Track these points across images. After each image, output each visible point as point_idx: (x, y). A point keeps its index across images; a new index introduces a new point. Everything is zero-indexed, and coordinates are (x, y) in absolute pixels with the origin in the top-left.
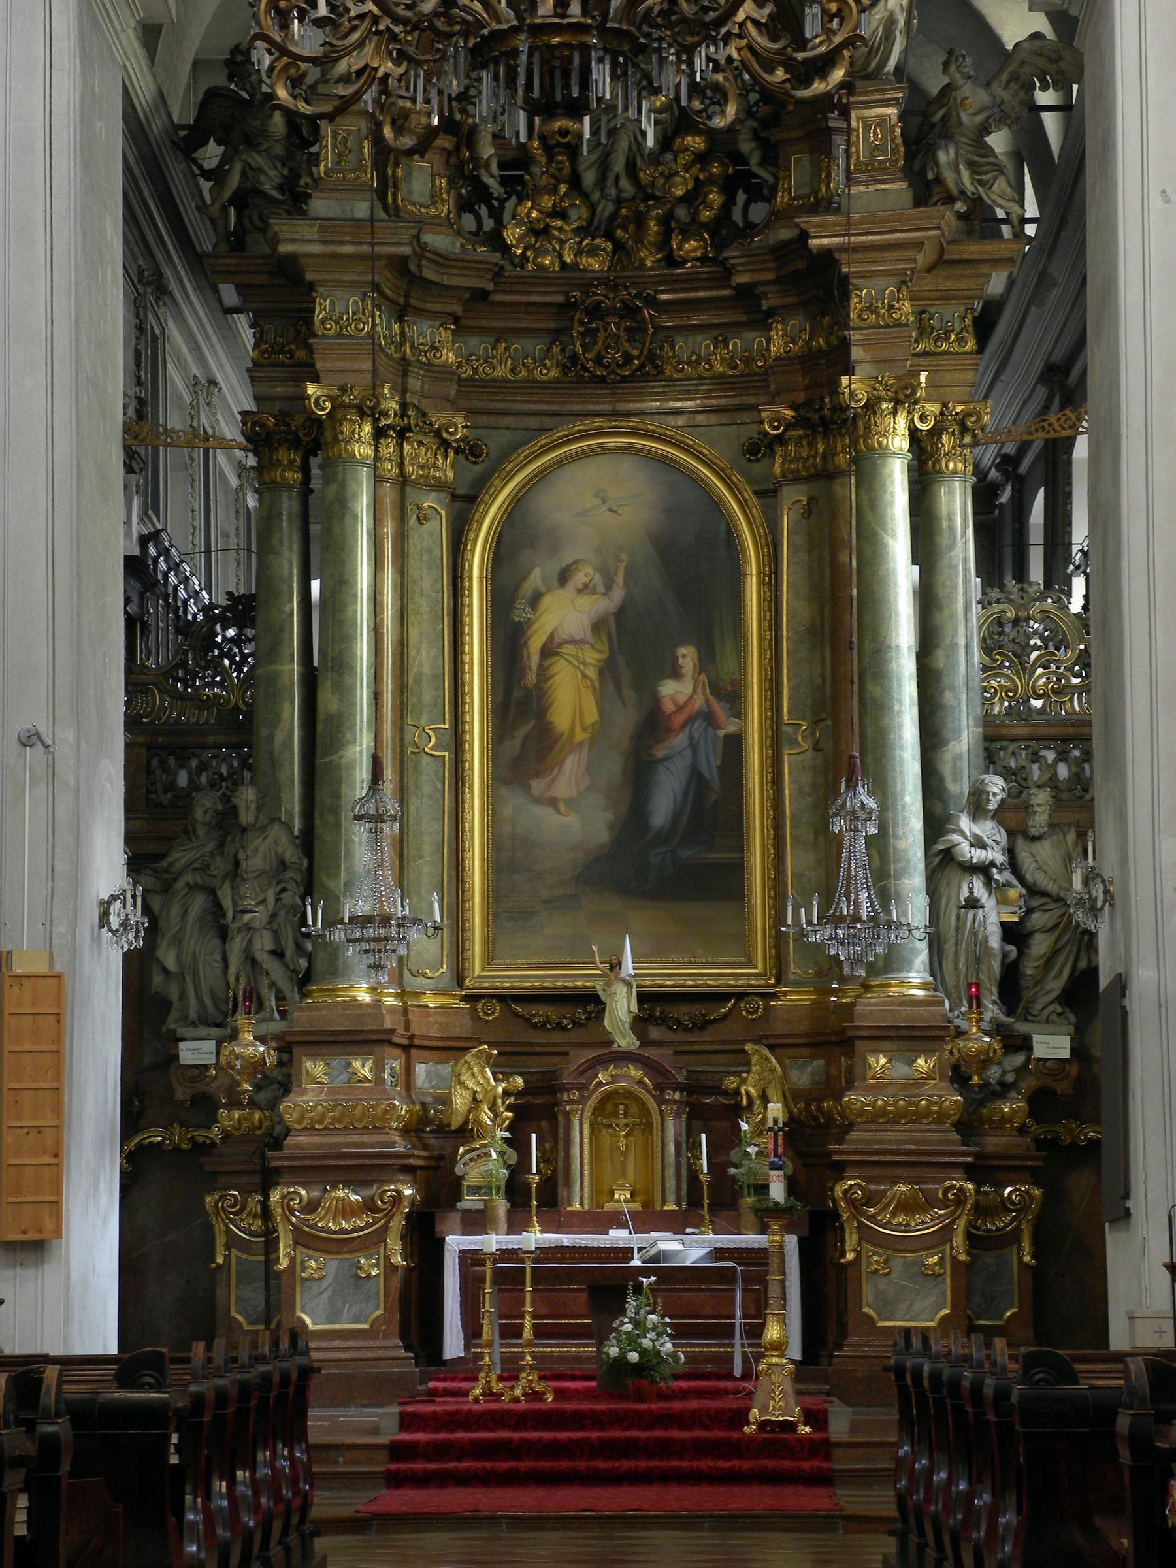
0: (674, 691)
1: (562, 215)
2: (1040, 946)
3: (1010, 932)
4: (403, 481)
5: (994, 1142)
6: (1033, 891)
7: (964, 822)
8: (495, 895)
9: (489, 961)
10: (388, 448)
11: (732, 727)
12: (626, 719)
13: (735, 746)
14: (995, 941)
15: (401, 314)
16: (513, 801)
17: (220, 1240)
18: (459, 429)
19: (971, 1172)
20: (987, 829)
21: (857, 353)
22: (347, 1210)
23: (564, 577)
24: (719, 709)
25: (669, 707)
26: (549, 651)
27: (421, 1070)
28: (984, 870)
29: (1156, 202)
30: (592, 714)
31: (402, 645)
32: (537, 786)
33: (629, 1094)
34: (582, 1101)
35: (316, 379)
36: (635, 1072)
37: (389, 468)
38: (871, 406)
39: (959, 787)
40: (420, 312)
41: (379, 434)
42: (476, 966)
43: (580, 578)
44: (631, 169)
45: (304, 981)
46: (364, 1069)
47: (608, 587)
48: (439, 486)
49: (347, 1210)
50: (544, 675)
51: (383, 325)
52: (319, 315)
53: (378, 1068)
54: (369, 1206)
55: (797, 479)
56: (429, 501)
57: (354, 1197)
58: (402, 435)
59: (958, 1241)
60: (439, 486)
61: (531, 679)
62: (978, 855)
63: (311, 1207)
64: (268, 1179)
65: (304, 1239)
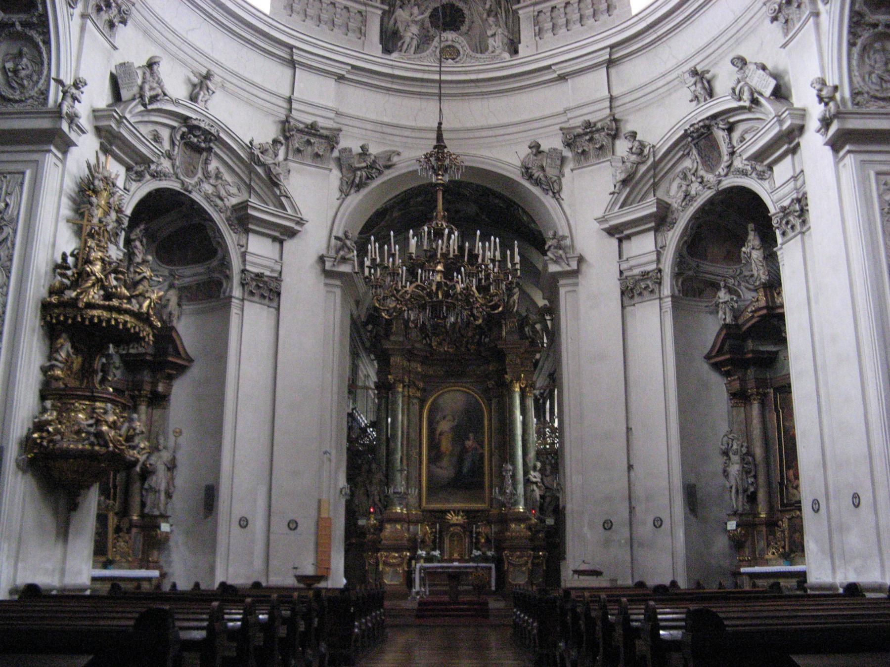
0: (469, 443)
1: (444, 340)
2: (548, 500)
3: (542, 497)
4: (409, 396)
5: (537, 543)
6: (547, 488)
7: (532, 473)
8: (429, 489)
9: (427, 503)
10: (406, 390)
11: (481, 451)
12: (458, 448)
13: (482, 456)
14: (538, 498)
15: (409, 361)
16: (433, 467)
17: (367, 564)
18: (421, 385)
19: (533, 549)
20: (537, 474)
21: (508, 370)
22: (395, 558)
23: (444, 418)
24: (478, 447)
25: (467, 447)
26: (440, 434)
27: (411, 527)
28: (536, 483)
29: (569, 340)
30: (451, 448)
31: (408, 432)
32: (438, 464)
33: (457, 533)
34: (447, 534)
35: (390, 374)
36: (459, 528)
37: (406, 393)
38: (512, 381)
39: (531, 465)
40: (415, 361)
41: (404, 386)
42: (424, 504)
43: (448, 418)
44: (460, 331)
45: (385, 507)
46: (399, 527)
47: (454, 419)
48: (416, 398)
49: (395, 558)
50: (440, 441)
51: (405, 363)
52: (391, 361)
53: (402, 527)
54: (400, 557)
55: (495, 397)
56: (415, 401)
57: (396, 555)
58: (409, 387)
59: (529, 565)
60: (416, 398)
61: (437, 441)
62: (534, 480)
63: (387, 557)
64: (378, 550)
65: (386, 564)
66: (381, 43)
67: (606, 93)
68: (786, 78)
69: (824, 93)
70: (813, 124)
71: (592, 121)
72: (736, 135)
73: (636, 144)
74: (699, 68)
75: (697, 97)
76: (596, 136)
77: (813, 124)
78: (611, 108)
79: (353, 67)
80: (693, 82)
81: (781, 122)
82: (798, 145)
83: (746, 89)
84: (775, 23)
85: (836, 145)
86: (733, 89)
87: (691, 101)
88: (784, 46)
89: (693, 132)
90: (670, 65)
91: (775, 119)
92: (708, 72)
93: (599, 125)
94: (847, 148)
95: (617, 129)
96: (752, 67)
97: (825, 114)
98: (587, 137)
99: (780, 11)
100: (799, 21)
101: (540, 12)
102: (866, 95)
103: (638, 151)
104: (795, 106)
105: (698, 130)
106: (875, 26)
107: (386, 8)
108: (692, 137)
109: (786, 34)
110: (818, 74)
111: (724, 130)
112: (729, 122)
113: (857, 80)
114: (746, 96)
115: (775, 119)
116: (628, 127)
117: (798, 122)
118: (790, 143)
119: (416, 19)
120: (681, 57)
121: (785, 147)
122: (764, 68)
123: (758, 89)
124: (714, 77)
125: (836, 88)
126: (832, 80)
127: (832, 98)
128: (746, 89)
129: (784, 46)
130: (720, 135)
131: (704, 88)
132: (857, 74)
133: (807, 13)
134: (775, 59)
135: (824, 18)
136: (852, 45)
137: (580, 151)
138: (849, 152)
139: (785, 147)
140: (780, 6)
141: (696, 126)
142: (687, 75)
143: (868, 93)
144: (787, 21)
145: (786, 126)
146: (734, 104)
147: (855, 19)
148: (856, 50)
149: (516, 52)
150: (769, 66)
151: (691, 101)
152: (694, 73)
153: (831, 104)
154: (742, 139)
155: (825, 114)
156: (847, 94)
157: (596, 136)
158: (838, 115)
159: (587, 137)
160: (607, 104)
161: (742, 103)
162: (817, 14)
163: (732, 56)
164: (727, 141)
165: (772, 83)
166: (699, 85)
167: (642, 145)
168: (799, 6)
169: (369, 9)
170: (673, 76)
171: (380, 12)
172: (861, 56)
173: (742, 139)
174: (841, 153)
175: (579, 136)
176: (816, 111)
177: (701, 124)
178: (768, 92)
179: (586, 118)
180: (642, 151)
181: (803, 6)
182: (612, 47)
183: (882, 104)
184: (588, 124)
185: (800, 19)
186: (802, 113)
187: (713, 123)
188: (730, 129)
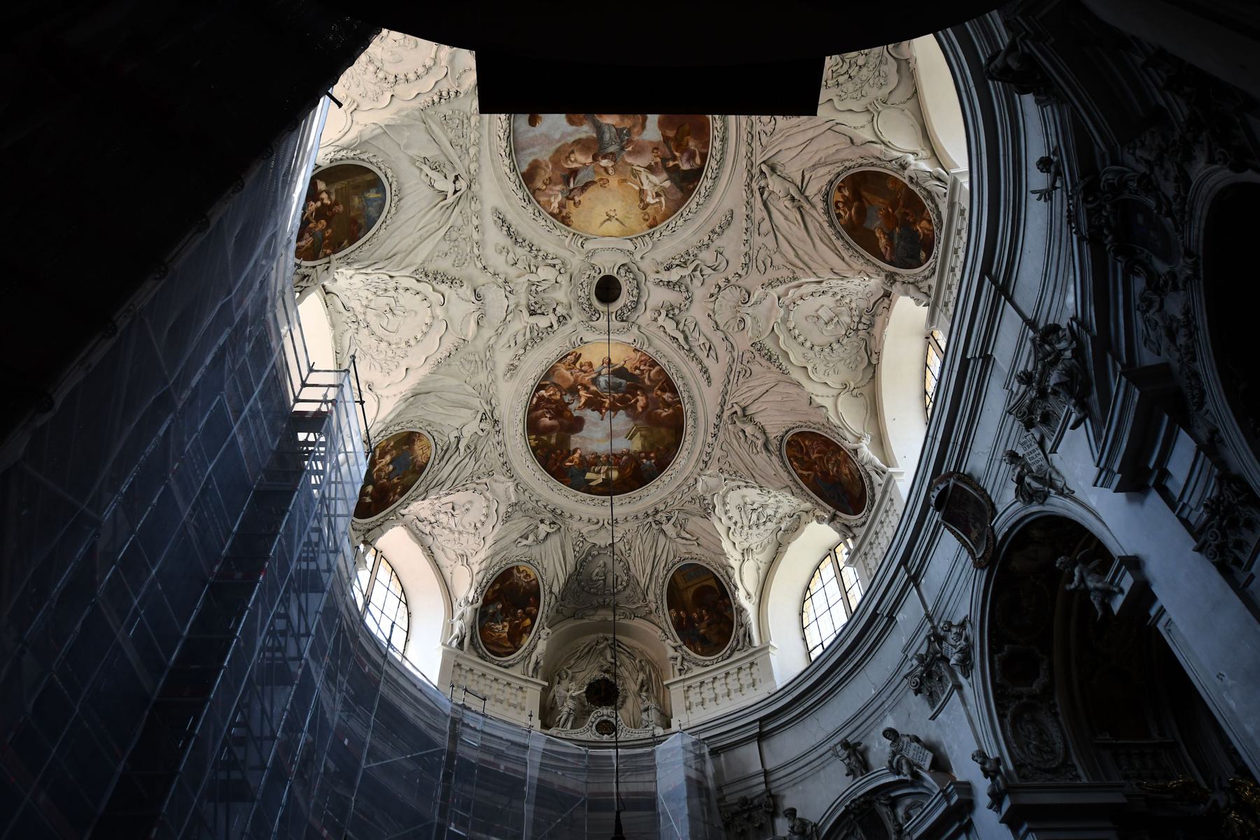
66: (540, 719)
67: (760, 768)
68: (942, 749)
69: (987, 766)
70: (983, 798)
71: (749, 797)
72: (900, 812)
73: (797, 823)
74: (849, 739)
75: (852, 770)
76: (754, 813)
77: (983, 798)
78: (766, 783)
79: (513, 743)
80: (845, 755)
81: (947, 797)
82: (970, 822)
83: (904, 761)
84: (919, 695)
85: (1012, 821)
86: (891, 762)
87: (847, 775)
88: (933, 718)
89: (854, 808)
90: (821, 736)
91: (941, 794)
92: (859, 744)
93: (756, 802)
94: (1026, 826)
95: (776, 806)
96: (906, 740)
97: (994, 789)
98: (746, 816)
99: (922, 684)
100: (943, 693)
101: (689, 687)
102: (1029, 767)
103: (800, 830)
104: (958, 779)
105: (859, 806)
106: (1019, 697)
107: (546, 684)
108: (854, 814)
109: (933, 706)
110: (976, 748)
111: (886, 805)
112: (890, 797)
113: (1016, 751)
114: (905, 769)
115: (941, 794)
116: (788, 803)
117: (965, 797)
118: (961, 820)
119: (574, 695)
120: (830, 729)
121: (957, 825)
122: (917, 740)
123: (916, 762)
124: (866, 749)
125: (998, 761)
126: (992, 753)
127: (998, 772)
128: (904, 761)
129: (933, 718)
130: (884, 811)
131: (858, 761)
132: (1015, 745)
133: (951, 685)
134: (928, 731)
135: (967, 690)
136: (1001, 717)
137: (739, 831)
138: (1029, 830)
139: (957, 825)
140: (921, 678)
141: (857, 802)
142: (839, 748)
143: (1031, 765)
144: (931, 695)
145: (953, 802)
146: (892, 779)
147: (999, 691)
148: (1008, 720)
149: (669, 726)
150: (922, 738)
151: (847, 775)
152: (845, 745)
153: (998, 778)
154: (908, 817)
155: (994, 789)
156: (1010, 767)
157: (754, 813)
158: (1010, 790)
159: (746, 816)
160: (762, 779)
161: (902, 777)
162: (959, 687)
163: (881, 731)
164: (892, 817)
165: (930, 756)
166: (853, 758)
167: (803, 823)
168: (940, 680)
169: (530, 685)
170: (826, 748)
171: (540, 688)
172: (1013, 726)
173: (908, 817)
174: (1022, 832)
175: (737, 814)
176: (982, 786)
177: (862, 799)
178: (927, 765)
179: (743, 794)
180: (804, 831)
181: (944, 679)
182: (761, 720)
183: (1049, 776)
184: (744, 801)
185: (943, 692)
186: (968, 787)
187: (874, 798)
188: (894, 803)
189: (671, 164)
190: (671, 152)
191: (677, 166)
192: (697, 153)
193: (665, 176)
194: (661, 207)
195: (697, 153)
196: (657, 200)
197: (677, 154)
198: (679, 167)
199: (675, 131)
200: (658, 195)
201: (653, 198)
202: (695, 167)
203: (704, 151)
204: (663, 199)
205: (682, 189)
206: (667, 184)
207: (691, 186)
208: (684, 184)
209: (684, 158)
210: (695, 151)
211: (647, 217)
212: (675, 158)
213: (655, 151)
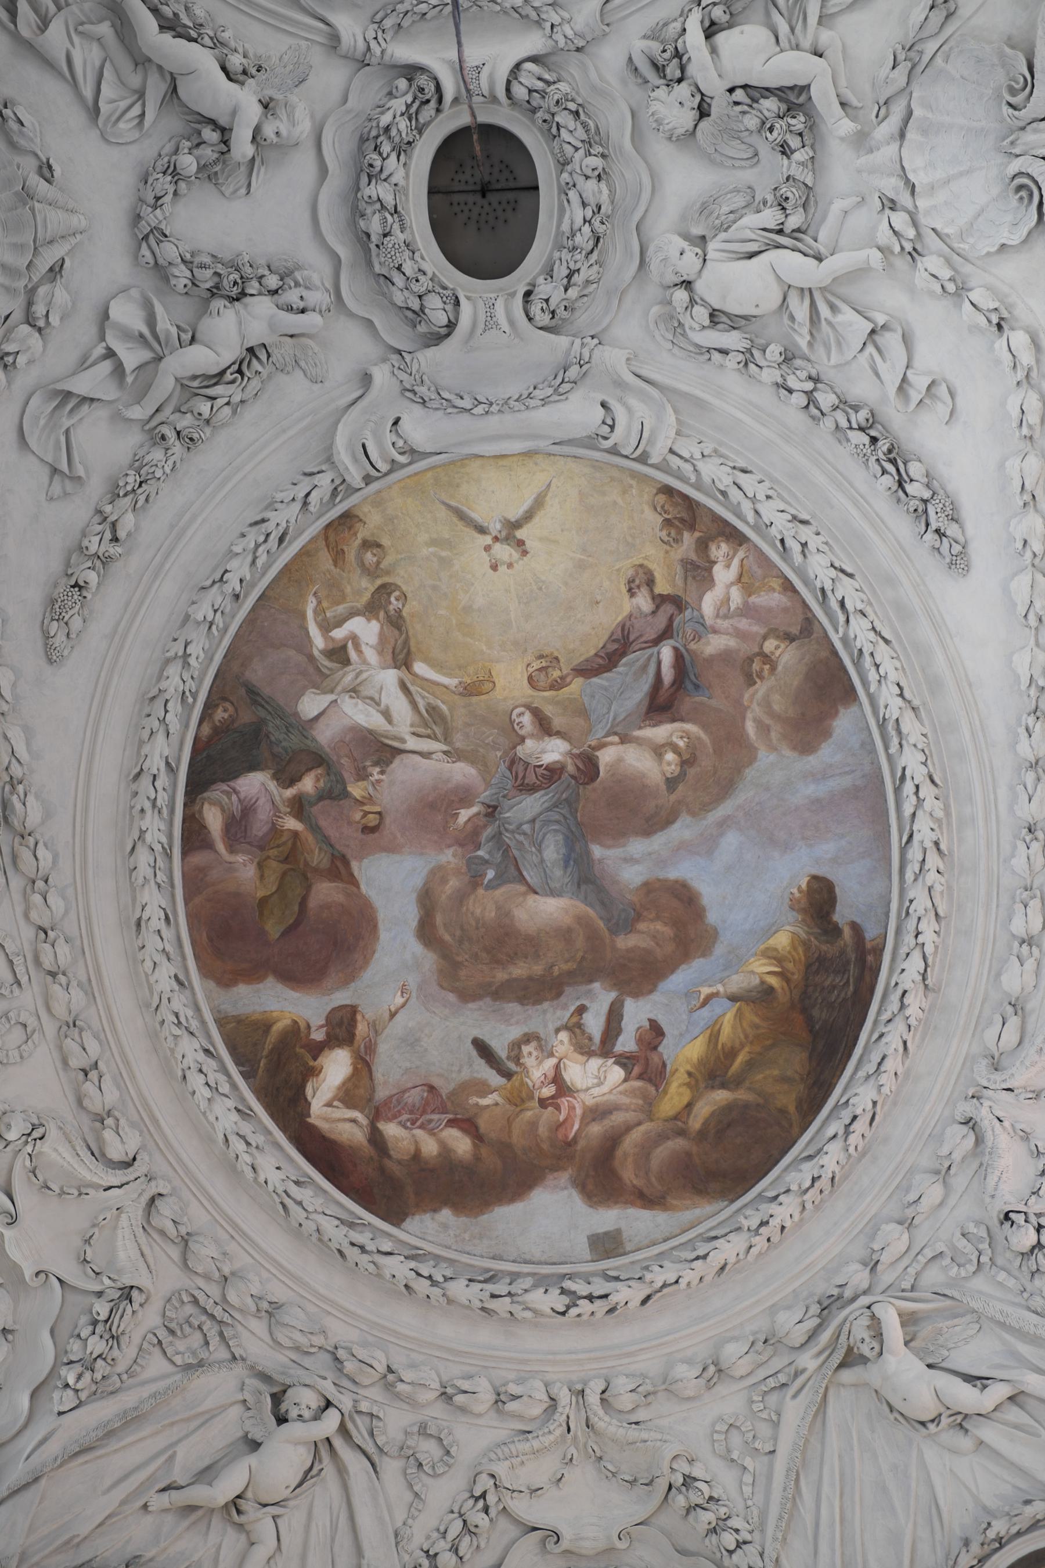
189: (308, 784)
190: (314, 828)
191: (287, 777)
192: (221, 847)
193: (325, 735)
194: (319, 611)
195: (221, 847)
196: (338, 634)
197: (292, 824)
198: (276, 777)
199: (312, 903)
200: (339, 654)
201: (354, 638)
202: (217, 792)
203: (199, 858)
204: (319, 642)
205: (253, 694)
206: (310, 705)
207: (220, 715)
208: (246, 717)
209: (263, 815)
210: (231, 850)
211: (369, 557)
212: (299, 807)
213: (372, 820)
